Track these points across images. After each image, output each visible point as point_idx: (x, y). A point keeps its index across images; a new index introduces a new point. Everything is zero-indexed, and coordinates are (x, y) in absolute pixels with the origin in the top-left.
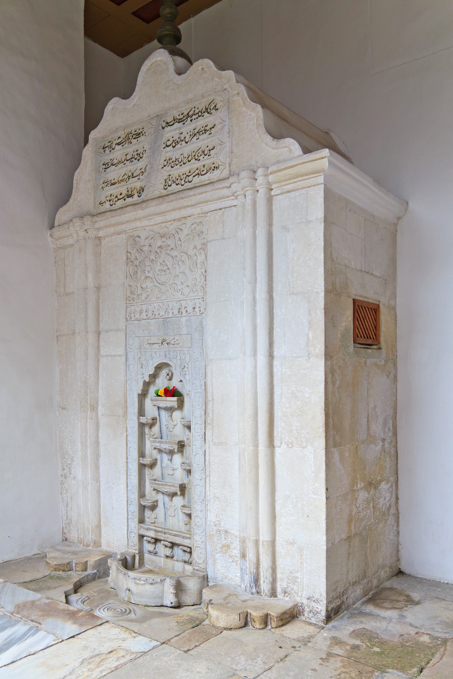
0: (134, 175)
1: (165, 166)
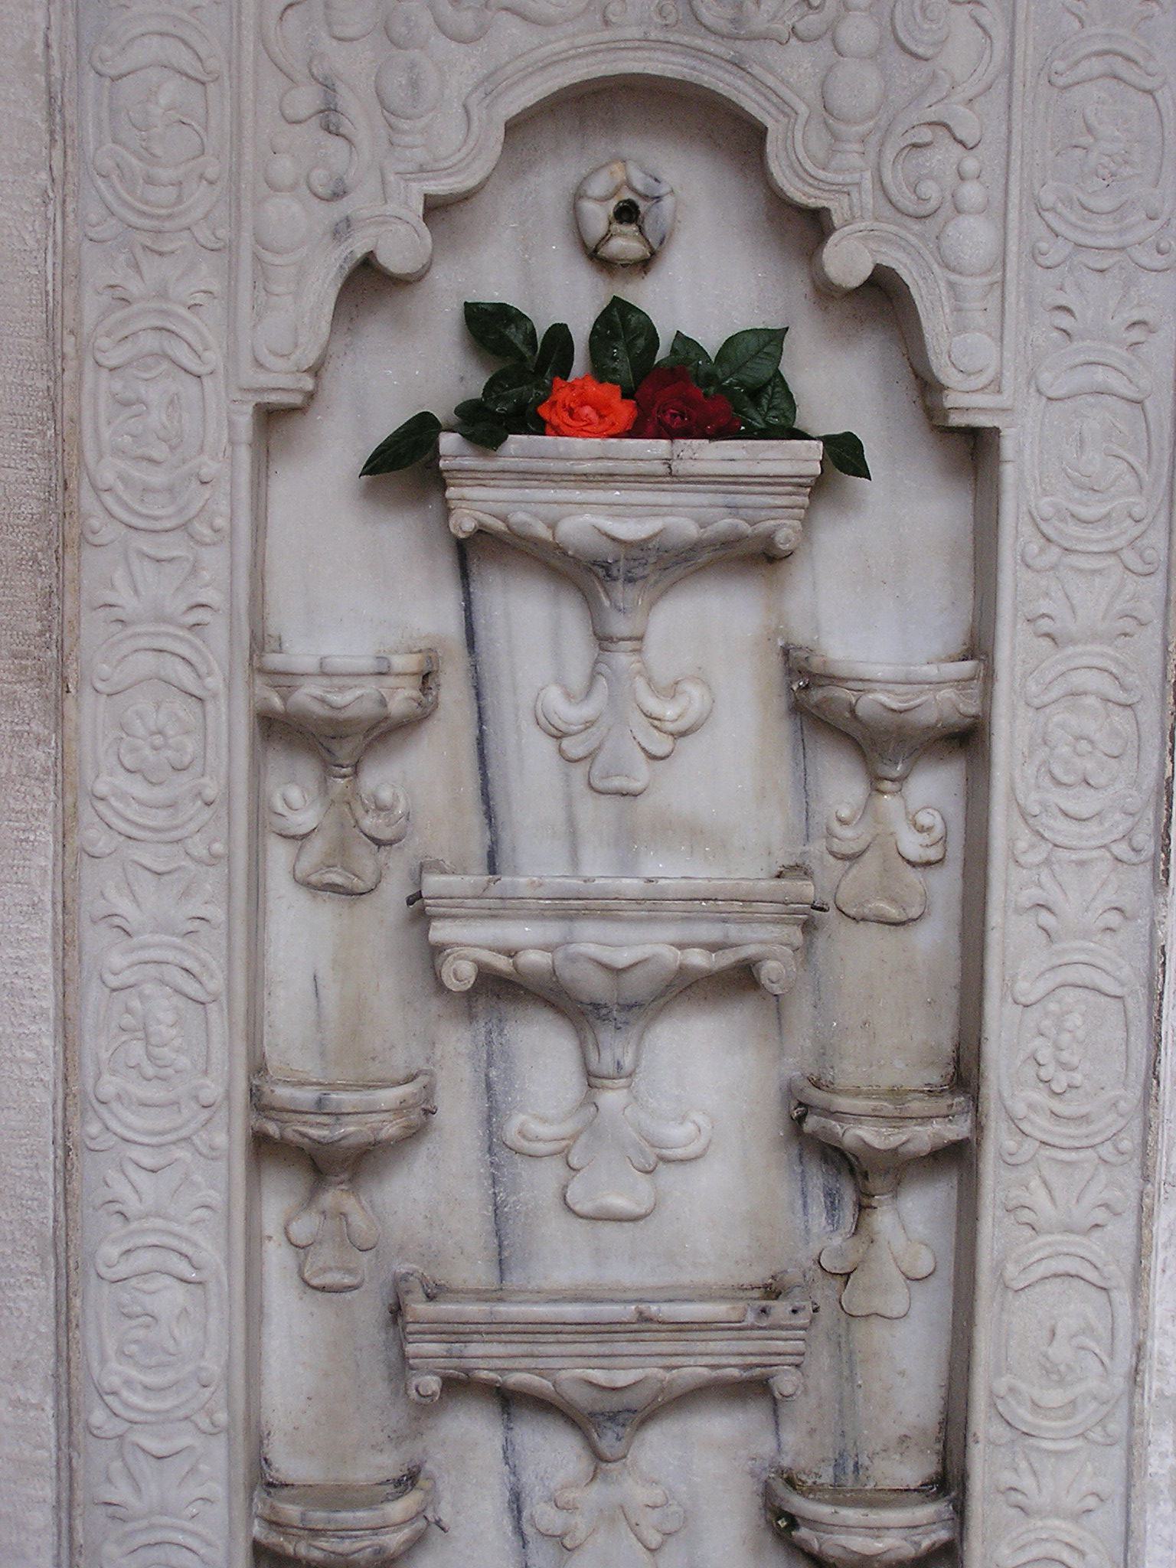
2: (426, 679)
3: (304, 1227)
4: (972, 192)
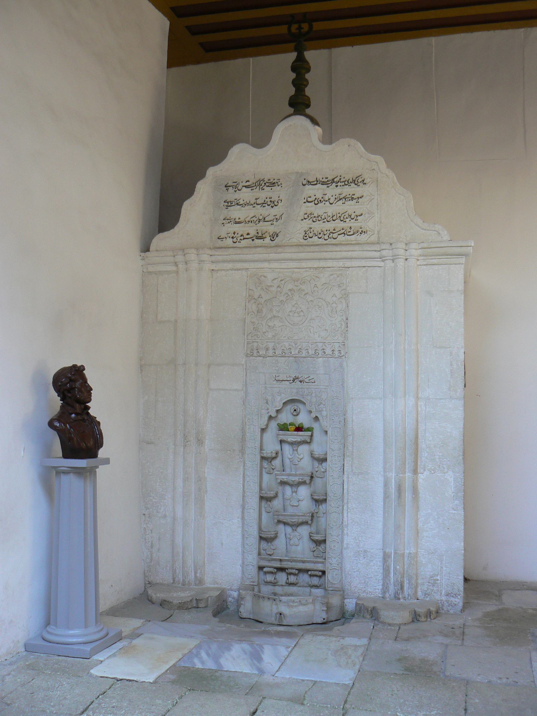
0: (266, 219)
1: (305, 219)
3: (266, 506)
4: (324, 409)
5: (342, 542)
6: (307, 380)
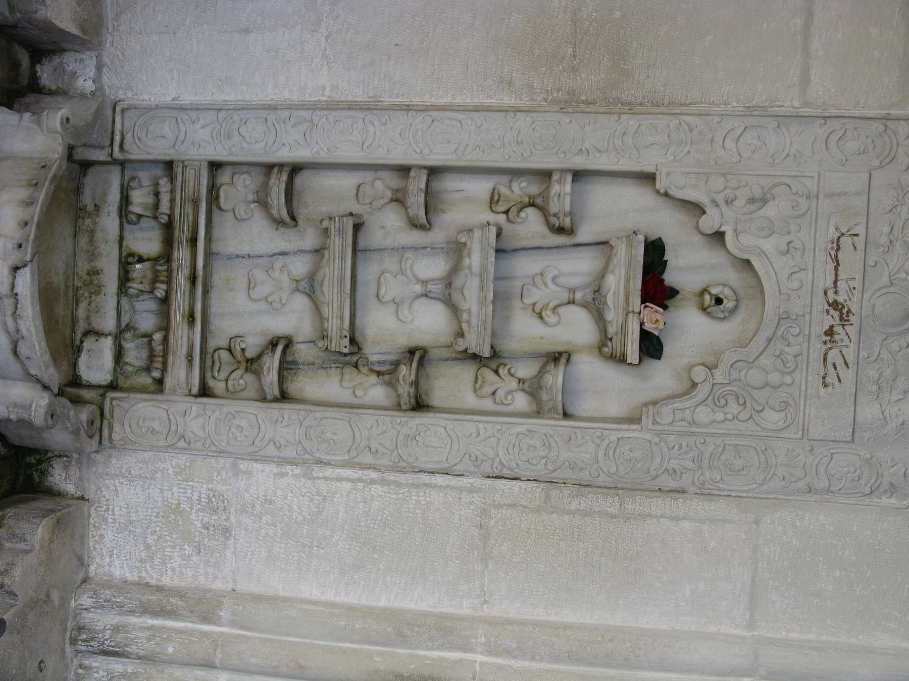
2: (561, 230)
5: (255, 458)
6: (833, 355)
